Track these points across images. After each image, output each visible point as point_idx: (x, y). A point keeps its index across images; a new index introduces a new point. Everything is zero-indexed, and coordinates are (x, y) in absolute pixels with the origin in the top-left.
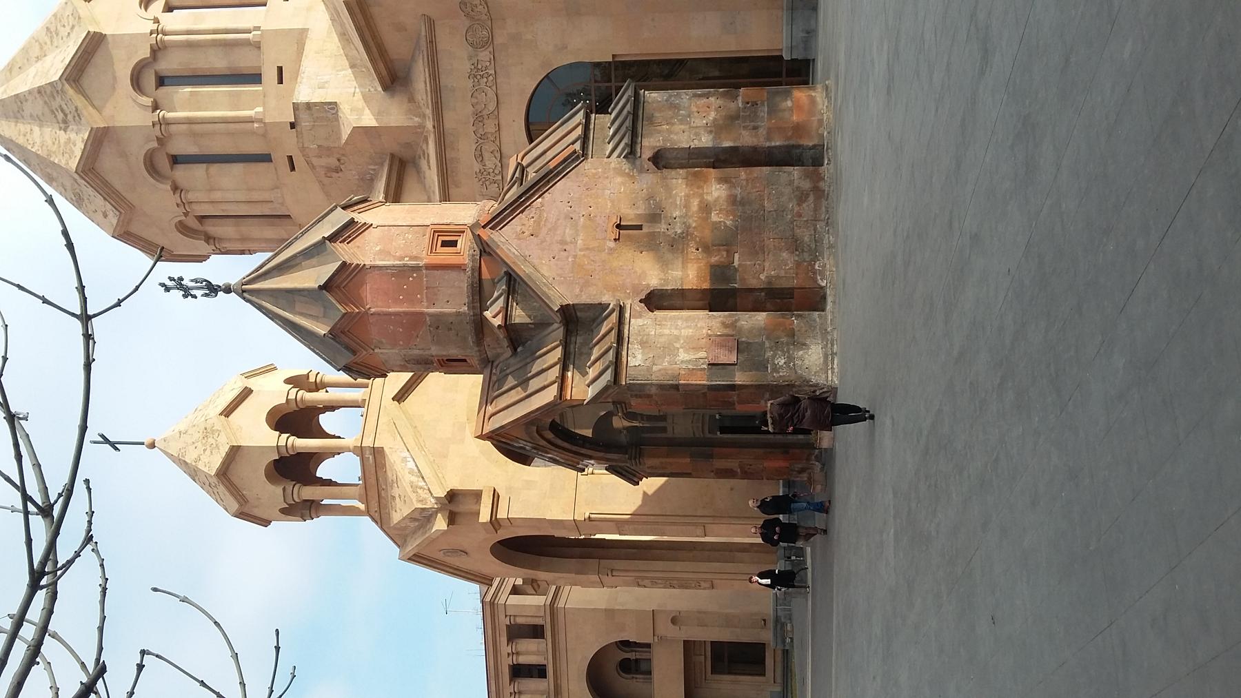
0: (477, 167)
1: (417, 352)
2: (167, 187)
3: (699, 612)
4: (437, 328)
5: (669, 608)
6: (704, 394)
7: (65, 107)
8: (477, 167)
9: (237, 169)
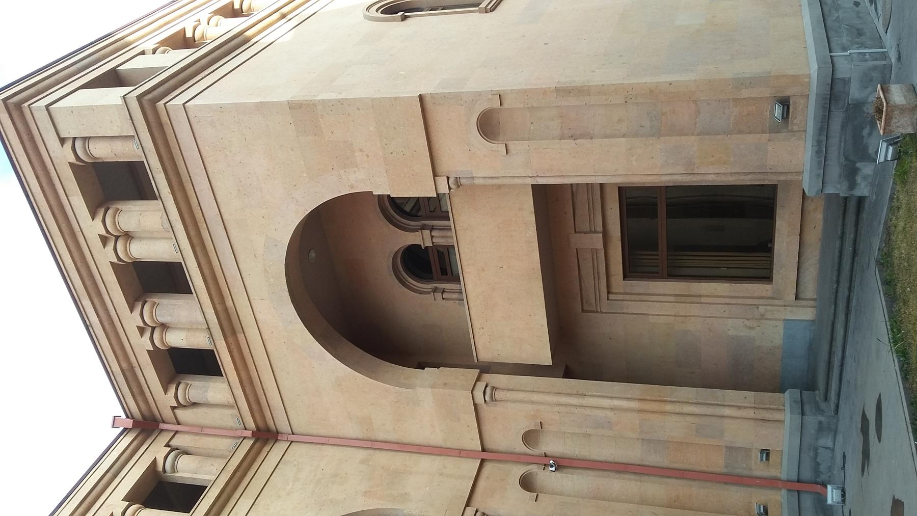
3: (563, 91)
5: (471, 86)
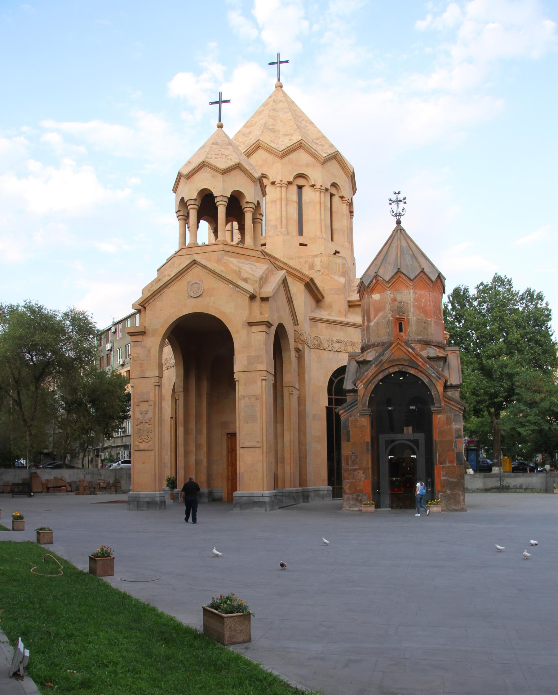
0: (335, 339)
1: (412, 309)
2: (291, 180)
4: (425, 323)
6: (454, 450)
7: (325, 148)
8: (335, 339)
9: (295, 216)
